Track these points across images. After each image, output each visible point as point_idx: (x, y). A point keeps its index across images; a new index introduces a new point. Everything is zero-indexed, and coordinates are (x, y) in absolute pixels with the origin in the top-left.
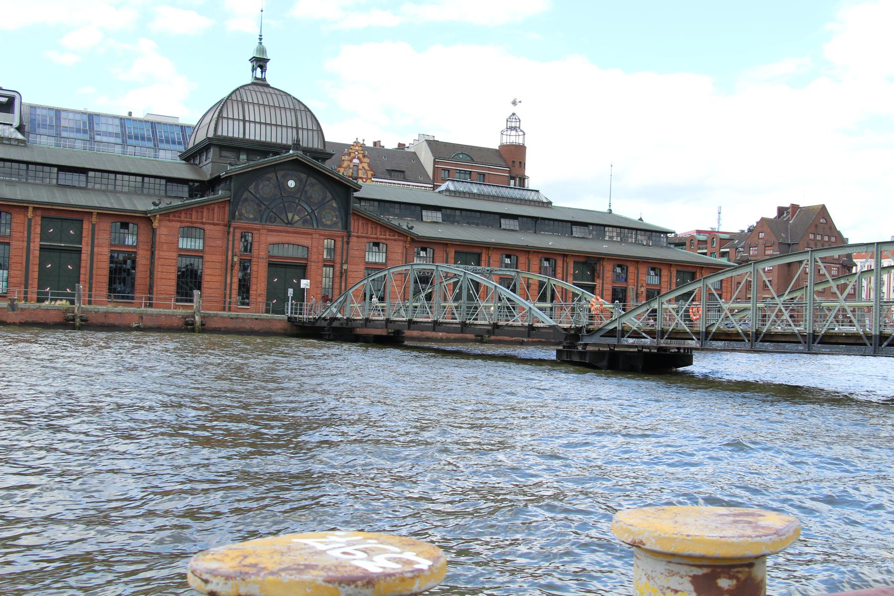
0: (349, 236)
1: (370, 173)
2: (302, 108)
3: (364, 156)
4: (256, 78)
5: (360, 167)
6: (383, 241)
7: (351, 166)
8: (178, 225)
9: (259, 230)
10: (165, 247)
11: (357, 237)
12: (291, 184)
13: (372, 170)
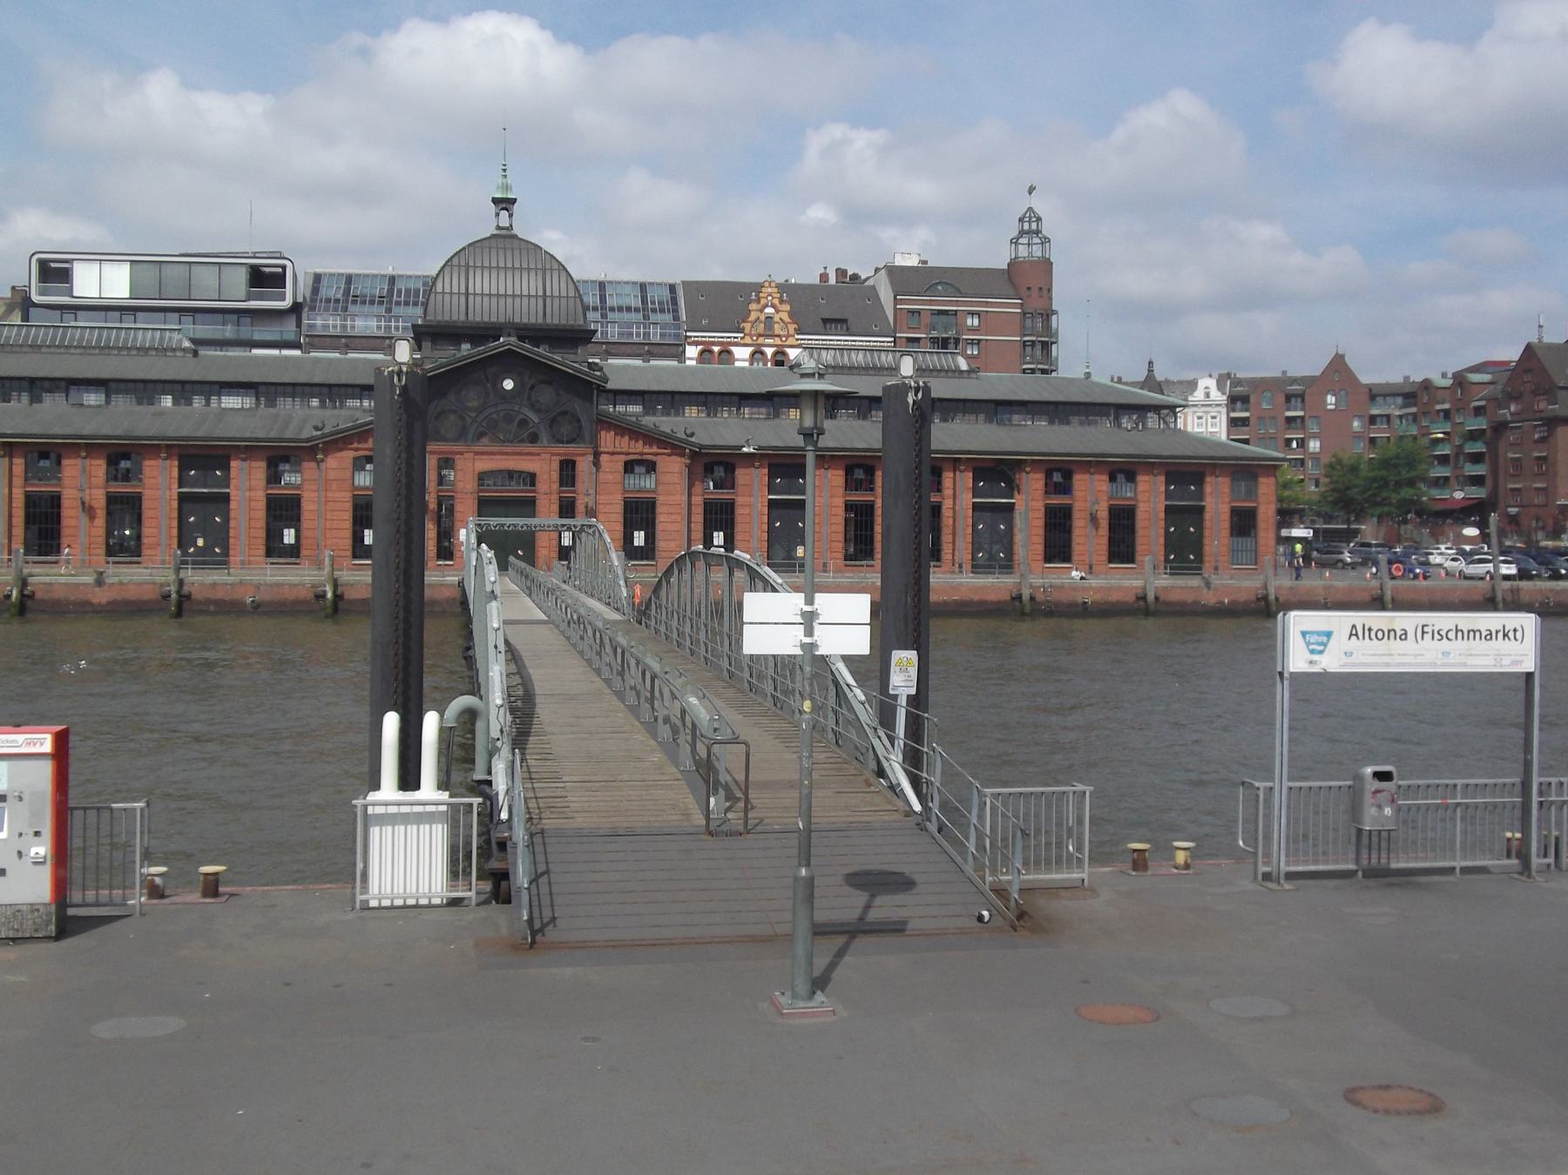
0: (597, 455)
1: (792, 327)
2: (555, 266)
3: (782, 302)
4: (498, 228)
5: (777, 319)
6: (649, 457)
7: (762, 318)
8: (352, 454)
9: (461, 453)
10: (334, 486)
12: (508, 385)
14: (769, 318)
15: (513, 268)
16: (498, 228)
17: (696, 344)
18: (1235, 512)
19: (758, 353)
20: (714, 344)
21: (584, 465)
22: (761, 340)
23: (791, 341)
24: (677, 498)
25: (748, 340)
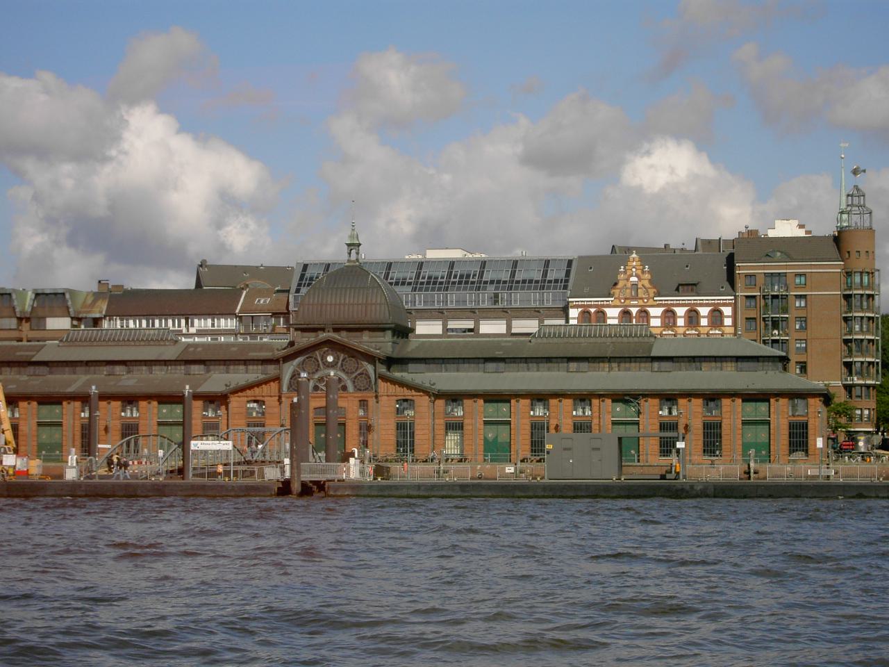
1: (652, 291)
3: (643, 272)
6: (410, 398)
7: (629, 285)
11: (388, 396)
13: (655, 287)
14: (635, 285)
15: (351, 288)
16: (349, 261)
17: (577, 307)
18: (792, 426)
19: (626, 314)
20: (591, 306)
21: (372, 402)
22: (628, 302)
23: (651, 302)
24: (427, 420)
25: (618, 303)
